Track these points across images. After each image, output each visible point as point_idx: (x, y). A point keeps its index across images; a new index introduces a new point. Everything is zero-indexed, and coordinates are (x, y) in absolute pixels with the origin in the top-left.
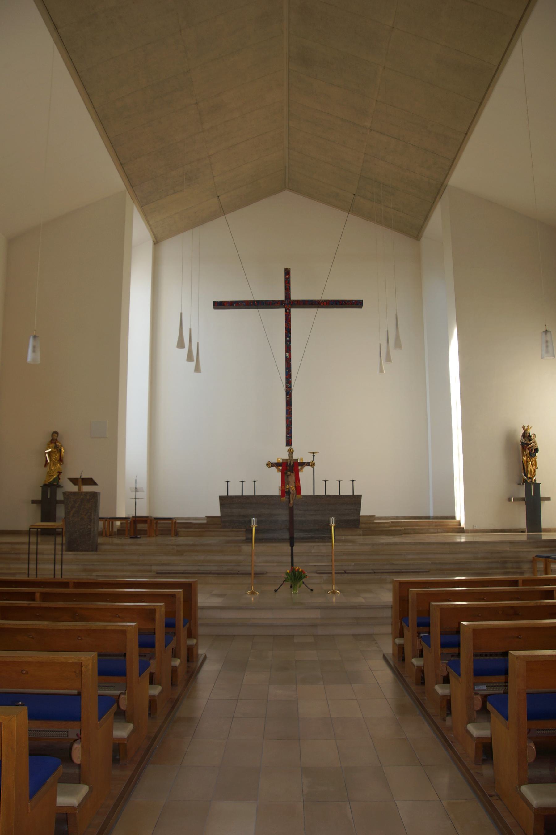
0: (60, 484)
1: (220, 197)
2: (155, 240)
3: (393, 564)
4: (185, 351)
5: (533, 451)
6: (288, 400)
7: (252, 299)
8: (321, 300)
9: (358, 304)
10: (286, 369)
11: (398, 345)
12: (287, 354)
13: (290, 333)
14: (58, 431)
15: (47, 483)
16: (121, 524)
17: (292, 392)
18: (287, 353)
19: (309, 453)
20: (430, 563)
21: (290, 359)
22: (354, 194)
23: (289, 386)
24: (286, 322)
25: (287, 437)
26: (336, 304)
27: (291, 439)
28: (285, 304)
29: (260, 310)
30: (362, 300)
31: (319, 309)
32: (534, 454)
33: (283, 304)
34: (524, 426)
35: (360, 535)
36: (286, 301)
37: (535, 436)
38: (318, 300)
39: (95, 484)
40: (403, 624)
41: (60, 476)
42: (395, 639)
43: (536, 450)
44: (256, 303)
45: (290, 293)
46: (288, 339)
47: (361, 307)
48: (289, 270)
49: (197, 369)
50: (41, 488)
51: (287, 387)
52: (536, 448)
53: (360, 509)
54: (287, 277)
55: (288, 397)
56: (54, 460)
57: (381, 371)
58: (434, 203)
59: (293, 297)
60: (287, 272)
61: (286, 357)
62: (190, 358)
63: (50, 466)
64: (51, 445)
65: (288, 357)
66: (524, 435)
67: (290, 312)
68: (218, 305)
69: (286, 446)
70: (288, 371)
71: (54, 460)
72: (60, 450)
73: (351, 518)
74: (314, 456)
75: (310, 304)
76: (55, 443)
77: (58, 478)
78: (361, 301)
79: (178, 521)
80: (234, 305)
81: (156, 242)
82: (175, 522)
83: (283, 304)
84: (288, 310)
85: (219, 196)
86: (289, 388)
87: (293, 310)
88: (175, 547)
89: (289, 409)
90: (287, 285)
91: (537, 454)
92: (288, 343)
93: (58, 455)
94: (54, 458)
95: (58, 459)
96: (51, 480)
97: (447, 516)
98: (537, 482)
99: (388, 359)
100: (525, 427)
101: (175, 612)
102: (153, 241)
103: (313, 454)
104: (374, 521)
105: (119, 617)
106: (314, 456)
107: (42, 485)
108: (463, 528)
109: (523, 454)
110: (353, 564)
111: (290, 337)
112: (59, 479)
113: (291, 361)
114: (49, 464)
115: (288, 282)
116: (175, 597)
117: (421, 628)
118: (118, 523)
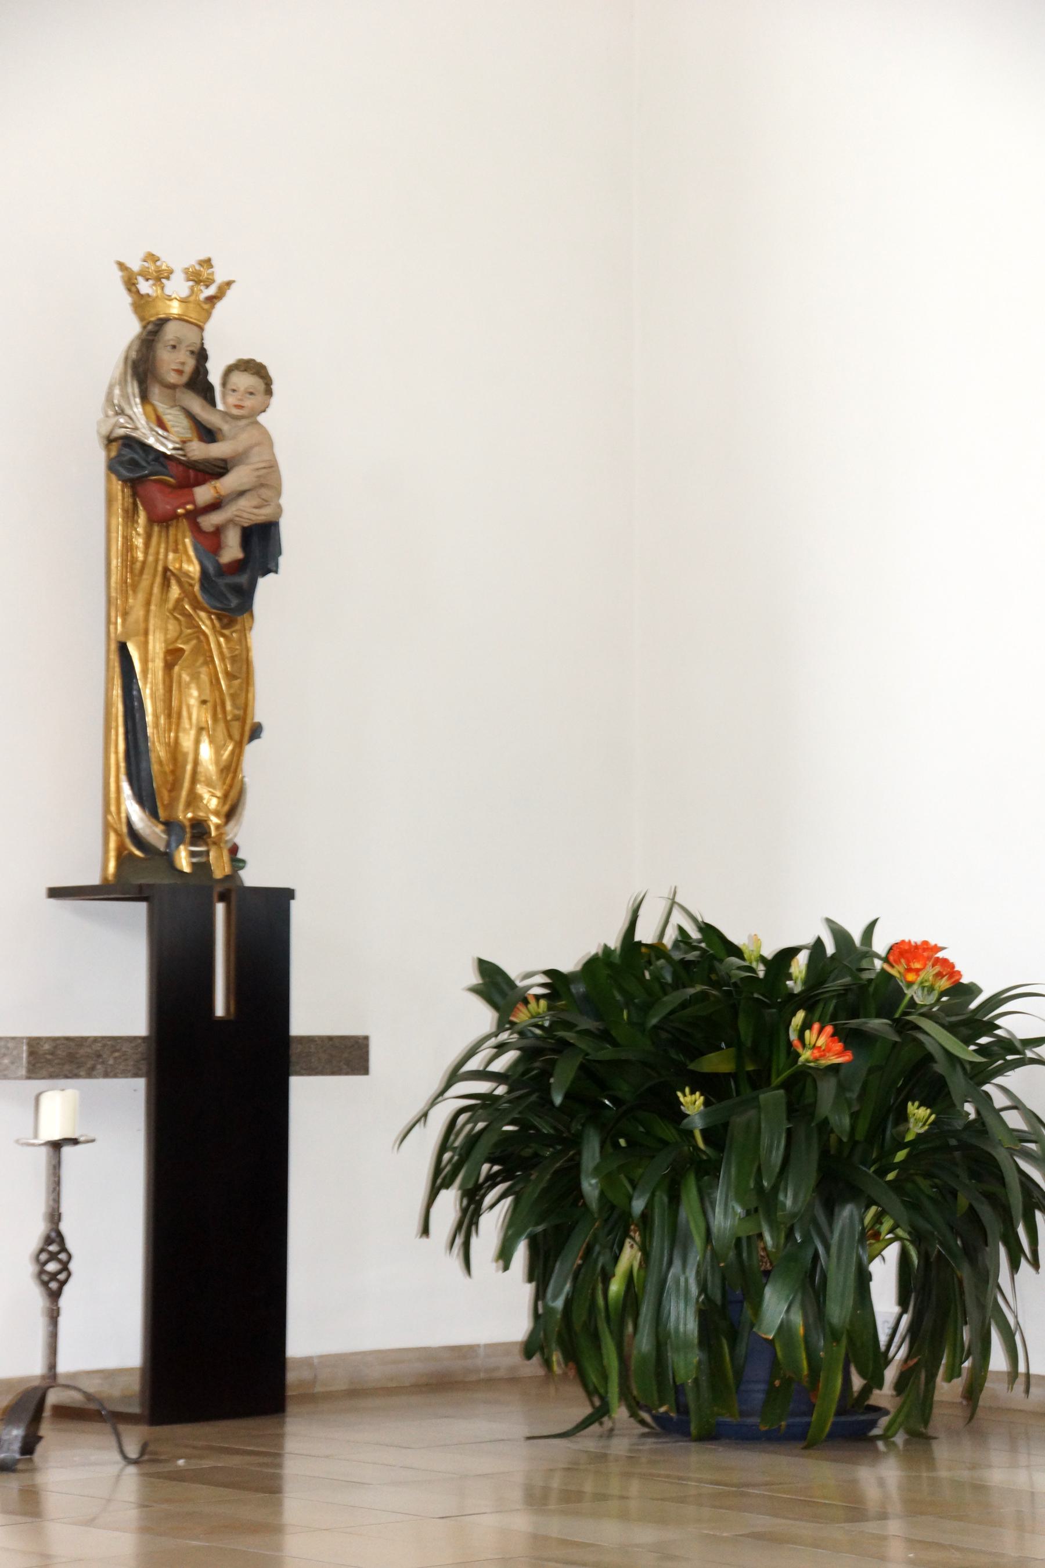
5: (232, 550)
32: (243, 579)
37: (269, 392)
52: (262, 515)
91: (265, 586)
98: (251, 877)
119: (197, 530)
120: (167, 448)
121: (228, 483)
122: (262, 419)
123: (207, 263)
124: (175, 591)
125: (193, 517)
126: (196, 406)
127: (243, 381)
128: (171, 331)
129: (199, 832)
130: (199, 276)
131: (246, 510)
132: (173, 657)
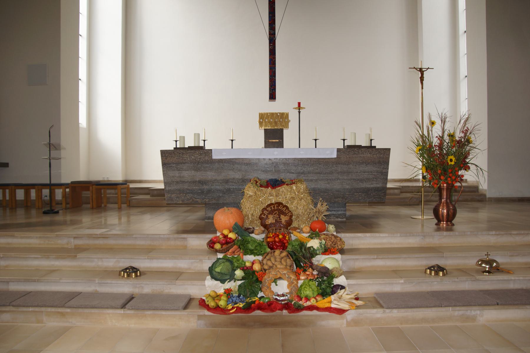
10: (270, 13)
17: (276, 40)
19: (295, 110)
25: (270, 89)
27: (275, 92)
51: (270, 34)
53: (388, 172)
70: (272, 16)
73: (372, 186)
74: (299, 112)
79: (132, 186)
86: (272, 34)
88: (72, 240)
89: (272, 58)
103: (298, 111)
106: (299, 112)
108: (485, 195)
110: (403, 281)
113: (275, 5)
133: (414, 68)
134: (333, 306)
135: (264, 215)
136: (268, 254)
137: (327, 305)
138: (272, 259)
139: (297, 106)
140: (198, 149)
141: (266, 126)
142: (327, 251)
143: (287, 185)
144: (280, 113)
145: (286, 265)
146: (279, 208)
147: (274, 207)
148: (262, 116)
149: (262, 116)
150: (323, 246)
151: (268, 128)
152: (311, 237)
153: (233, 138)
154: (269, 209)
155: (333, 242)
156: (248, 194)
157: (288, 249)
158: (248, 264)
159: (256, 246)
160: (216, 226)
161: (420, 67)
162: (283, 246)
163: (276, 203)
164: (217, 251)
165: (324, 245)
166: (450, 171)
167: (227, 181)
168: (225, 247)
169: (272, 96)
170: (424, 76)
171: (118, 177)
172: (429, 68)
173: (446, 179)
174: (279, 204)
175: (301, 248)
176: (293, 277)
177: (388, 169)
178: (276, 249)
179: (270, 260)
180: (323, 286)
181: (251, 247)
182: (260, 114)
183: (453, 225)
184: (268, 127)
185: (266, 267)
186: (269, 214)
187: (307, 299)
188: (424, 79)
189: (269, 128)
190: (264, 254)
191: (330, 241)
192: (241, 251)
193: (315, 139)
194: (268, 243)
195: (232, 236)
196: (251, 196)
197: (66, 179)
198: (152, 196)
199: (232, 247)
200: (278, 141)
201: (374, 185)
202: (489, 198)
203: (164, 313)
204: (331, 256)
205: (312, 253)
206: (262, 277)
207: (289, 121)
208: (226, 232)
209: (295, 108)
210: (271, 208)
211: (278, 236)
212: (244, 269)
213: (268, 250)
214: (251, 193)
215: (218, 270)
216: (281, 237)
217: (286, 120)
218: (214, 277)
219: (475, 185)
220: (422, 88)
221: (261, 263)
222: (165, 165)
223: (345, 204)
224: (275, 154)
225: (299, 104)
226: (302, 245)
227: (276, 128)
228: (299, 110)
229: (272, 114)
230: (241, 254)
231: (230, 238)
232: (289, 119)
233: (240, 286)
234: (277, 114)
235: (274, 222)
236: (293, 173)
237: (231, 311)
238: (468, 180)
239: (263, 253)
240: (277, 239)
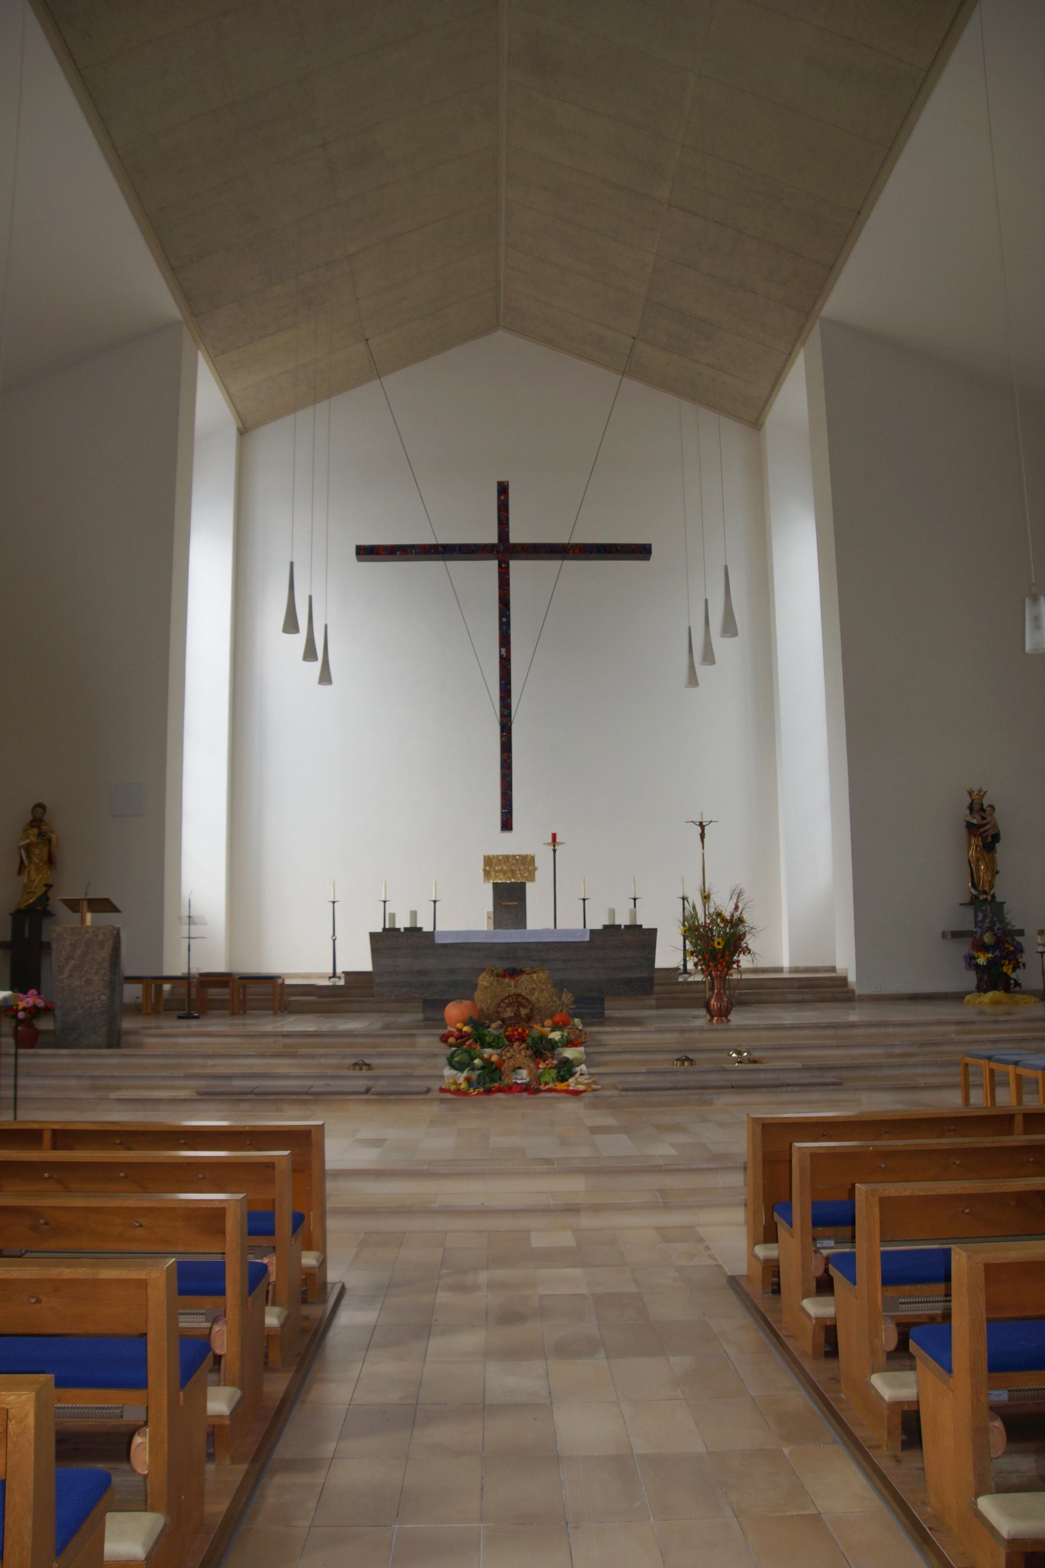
0: (49, 908)
1: (369, 342)
2: (241, 426)
3: (725, 1070)
4: (299, 640)
5: (989, 839)
6: (505, 740)
7: (433, 542)
8: (569, 544)
9: (642, 552)
11: (730, 628)
12: (503, 650)
13: (509, 609)
14: (46, 803)
15: (23, 906)
16: (173, 988)
18: (503, 647)
19: (544, 846)
20: (800, 1066)
21: (509, 660)
22: (634, 338)
23: (506, 712)
24: (500, 588)
26: (599, 552)
28: (498, 552)
29: (449, 563)
30: (650, 545)
31: (565, 562)
33: (495, 552)
34: (971, 789)
35: (651, 1008)
36: (501, 546)
38: (563, 544)
39: (115, 909)
40: (777, 1217)
41: (50, 894)
42: (754, 1246)
43: (996, 837)
44: (440, 548)
45: (507, 529)
46: (504, 620)
47: (648, 559)
48: (506, 484)
49: (325, 677)
50: (10, 917)
51: (502, 715)
52: (994, 833)
54: (502, 498)
55: (504, 734)
56: (37, 861)
57: (693, 680)
58: (790, 354)
59: (516, 537)
60: (503, 489)
61: (501, 657)
62: (310, 653)
63: (29, 872)
64: (30, 831)
65: (504, 656)
66: (971, 808)
67: (507, 569)
68: (366, 552)
69: (501, 832)
71: (37, 861)
72: (50, 840)
73: (635, 976)
74: (555, 851)
75: (547, 552)
76: (39, 827)
77: (45, 898)
78: (648, 546)
79: (288, 982)
80: (398, 553)
81: (244, 431)
82: (283, 984)
83: (495, 552)
84: (504, 563)
85: (367, 340)
86: (506, 716)
87: (513, 564)
88: (280, 1039)
89: (506, 758)
90: (501, 513)
91: (997, 845)
92: (504, 627)
93: (46, 850)
94: (37, 856)
95: (45, 857)
96: (31, 901)
97: (817, 967)
99: (709, 657)
100: (974, 791)
101: (274, 1200)
102: (238, 429)
103: (553, 848)
104: (678, 979)
105: (141, 1226)
106: (555, 851)
107: (12, 912)
108: (853, 992)
109: (970, 845)
111: (508, 617)
112: (48, 899)
113: (510, 664)
114: (27, 870)
115: (503, 509)
116: (274, 1168)
117: (819, 1229)
118: (167, 987)
119: (982, 837)
120: (975, 821)
121: (987, 827)
122: (994, 815)
123: (981, 789)
124: (978, 849)
125: (981, 834)
126: (982, 814)
127: (988, 809)
128: (975, 801)
129: (985, 892)
130: (980, 790)
131: (991, 832)
132: (978, 860)
133: (692, 822)
134: (571, 1088)
135: (502, 1008)
136: (506, 1047)
137: (565, 1088)
138: (511, 1050)
139: (550, 840)
140: (414, 931)
141: (496, 877)
142: (570, 1043)
143: (527, 974)
144: (519, 856)
145: (526, 1056)
146: (519, 1000)
147: (512, 999)
148: (488, 861)
149: (488, 861)
150: (564, 1038)
151: (499, 881)
152: (553, 1030)
153: (436, 898)
154: (507, 1001)
155: (576, 1036)
156: (482, 985)
157: (527, 1042)
158: (486, 1056)
159: (494, 1039)
160: (447, 1020)
161: (700, 821)
162: (522, 1039)
163: (515, 995)
164: (451, 1046)
165: (567, 1038)
166: (719, 956)
167: (452, 971)
168: (459, 1041)
169: (507, 824)
170: (706, 832)
171: (220, 966)
172: (711, 821)
173: (716, 966)
174: (518, 995)
175: (542, 1041)
176: (532, 1065)
177: (655, 954)
178: (515, 1041)
179: (508, 1051)
180: (562, 1073)
181: (488, 1039)
182: (485, 857)
183: (729, 1021)
184: (501, 879)
185: (504, 1058)
186: (507, 1006)
187: (546, 1083)
188: (706, 836)
189: (502, 882)
190: (502, 1047)
191: (574, 1034)
192: (478, 1044)
193: (583, 898)
194: (507, 1037)
195: (466, 1029)
196: (486, 988)
197: (177, 968)
198: (321, 996)
199: (467, 1040)
200: (516, 903)
201: (638, 974)
202: (859, 996)
203: (408, 1097)
204: (574, 1048)
205: (553, 1045)
206: (501, 1066)
207: (535, 869)
208: (459, 1025)
209: (548, 844)
210: (509, 1000)
211: (517, 1030)
212: (482, 1058)
213: (507, 1043)
214: (486, 984)
215: (456, 1059)
216: (520, 1030)
217: (531, 868)
218: (453, 1066)
219: (844, 975)
220: (703, 848)
221: (500, 1055)
222: (375, 950)
223: (603, 999)
224: (511, 936)
225: (554, 836)
226: (543, 1037)
227: (513, 880)
228: (554, 846)
229: (507, 858)
230: (478, 1048)
231: (466, 1032)
232: (536, 866)
233: (479, 1075)
234: (514, 857)
235: (513, 1015)
236: (535, 960)
237: (473, 1094)
238: (837, 968)
239: (501, 1045)
240: (515, 1033)
